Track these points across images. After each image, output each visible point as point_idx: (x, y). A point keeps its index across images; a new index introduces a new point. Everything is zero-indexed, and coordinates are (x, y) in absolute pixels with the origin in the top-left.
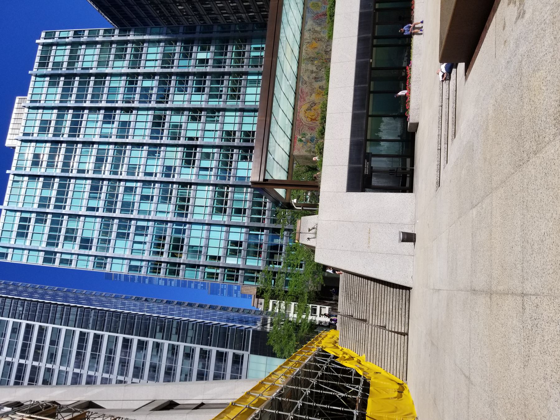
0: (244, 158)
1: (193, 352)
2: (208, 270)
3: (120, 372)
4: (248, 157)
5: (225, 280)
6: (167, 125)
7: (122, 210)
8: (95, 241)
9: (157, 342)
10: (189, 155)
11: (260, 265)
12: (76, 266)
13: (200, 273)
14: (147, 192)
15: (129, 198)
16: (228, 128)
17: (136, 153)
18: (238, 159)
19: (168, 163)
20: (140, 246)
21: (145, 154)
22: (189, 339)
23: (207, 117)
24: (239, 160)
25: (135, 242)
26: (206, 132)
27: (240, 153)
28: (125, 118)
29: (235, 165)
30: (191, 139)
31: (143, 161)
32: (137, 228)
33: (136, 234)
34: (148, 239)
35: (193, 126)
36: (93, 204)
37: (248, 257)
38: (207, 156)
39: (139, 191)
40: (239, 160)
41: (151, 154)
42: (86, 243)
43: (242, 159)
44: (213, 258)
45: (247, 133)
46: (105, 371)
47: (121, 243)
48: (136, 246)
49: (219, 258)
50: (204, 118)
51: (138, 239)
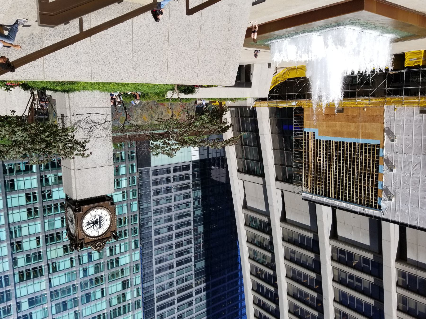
0: (50, 196)
1: (155, 200)
2: (131, 198)
3: (171, 239)
4: (48, 193)
5: (136, 184)
6: (28, 268)
7: (101, 272)
8: (123, 279)
9: (154, 224)
10: (52, 239)
11: (124, 165)
12: (140, 284)
13: (134, 203)
14: (85, 259)
15: (91, 271)
16: (24, 216)
17: (55, 282)
18: (52, 200)
19: (61, 252)
20: (123, 247)
21: (56, 275)
22: (149, 205)
23: (16, 236)
24: (52, 199)
25: (121, 252)
26: (30, 234)
27: (45, 200)
28: (25, 306)
29: (56, 201)
30: (38, 243)
31: (62, 274)
32: (111, 255)
33: (116, 254)
34: (118, 245)
35: (26, 246)
36: (99, 295)
37: (120, 174)
38: (52, 224)
39: (84, 266)
40: (52, 199)
41: (55, 270)
42: (125, 285)
43: (51, 197)
44: (124, 197)
45: (28, 198)
46: (172, 249)
47: (122, 262)
48: (123, 250)
49: (123, 192)
50: (17, 239)
51: (118, 251)
